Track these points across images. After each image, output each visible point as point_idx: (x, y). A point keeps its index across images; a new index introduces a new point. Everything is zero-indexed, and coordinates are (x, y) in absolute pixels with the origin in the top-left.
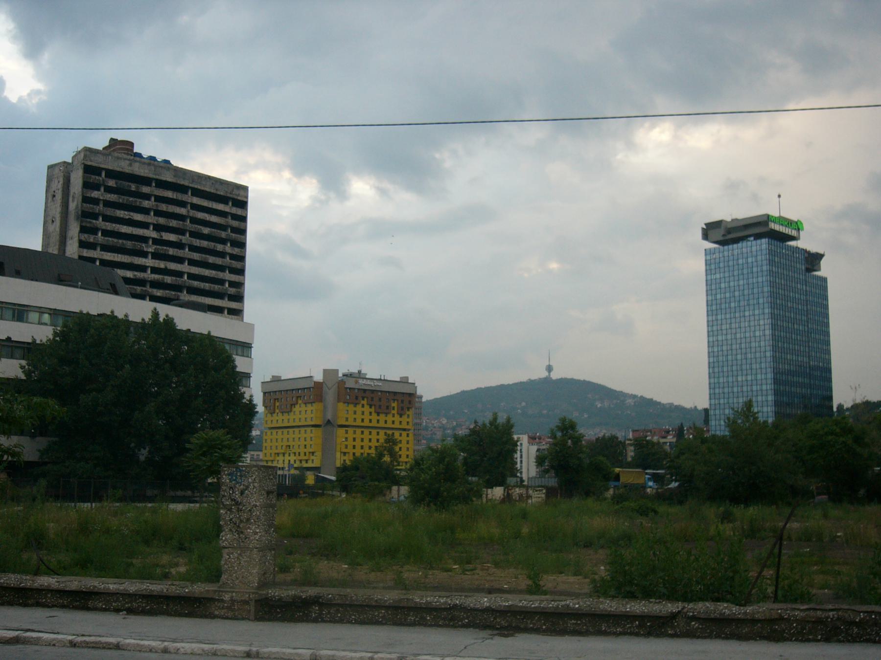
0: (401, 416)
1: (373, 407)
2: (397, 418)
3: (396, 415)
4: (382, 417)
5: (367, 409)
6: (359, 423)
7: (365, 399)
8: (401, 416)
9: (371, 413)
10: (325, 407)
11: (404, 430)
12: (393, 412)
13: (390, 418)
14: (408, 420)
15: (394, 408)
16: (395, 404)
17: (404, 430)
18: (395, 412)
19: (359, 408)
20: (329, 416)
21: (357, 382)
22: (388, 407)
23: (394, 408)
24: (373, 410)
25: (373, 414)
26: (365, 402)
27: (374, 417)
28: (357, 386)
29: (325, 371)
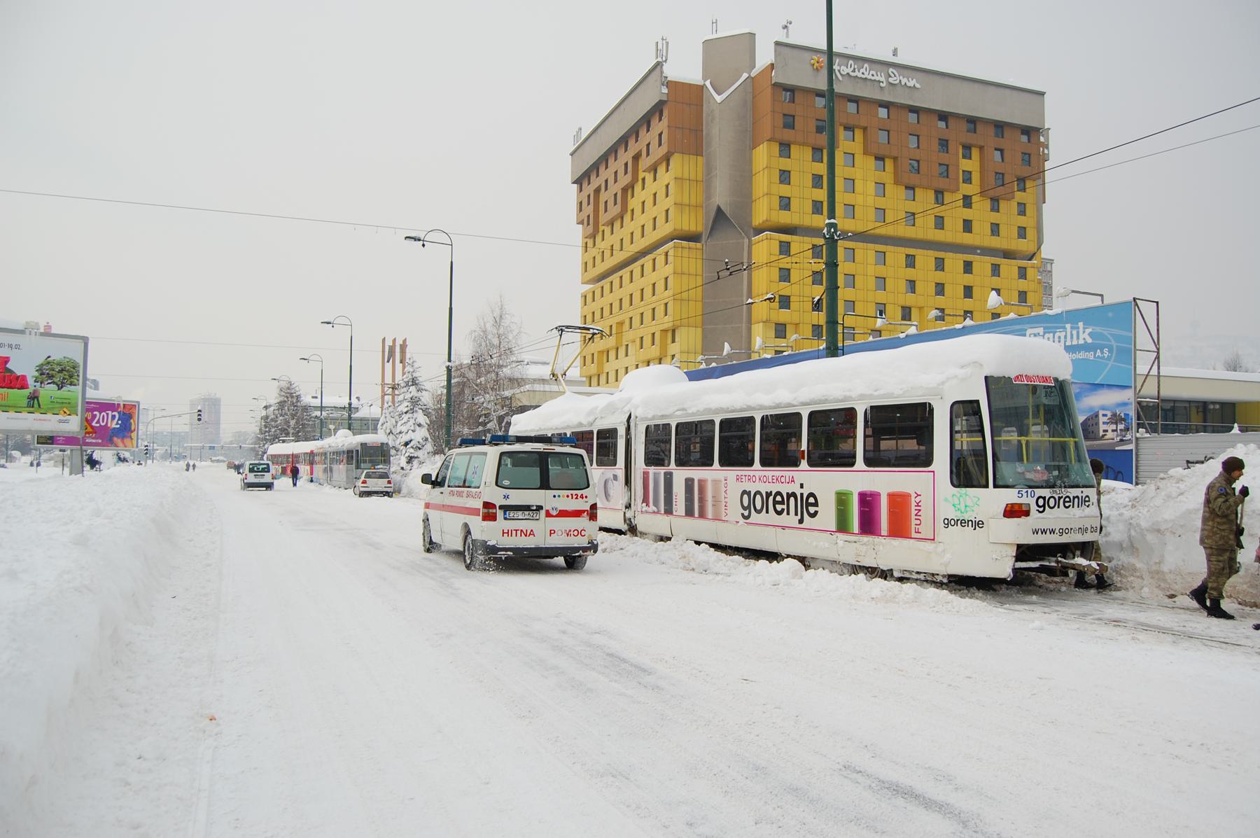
0: (995, 205)
1: (889, 164)
2: (981, 212)
7: (859, 134)
8: (995, 205)
9: (881, 186)
10: (709, 169)
11: (1008, 255)
12: (966, 189)
14: (1022, 221)
15: (968, 178)
17: (1008, 255)
18: (972, 189)
20: (721, 196)
22: (946, 170)
23: (968, 178)
24: (887, 176)
25: (890, 188)
27: (897, 201)
29: (712, 48)
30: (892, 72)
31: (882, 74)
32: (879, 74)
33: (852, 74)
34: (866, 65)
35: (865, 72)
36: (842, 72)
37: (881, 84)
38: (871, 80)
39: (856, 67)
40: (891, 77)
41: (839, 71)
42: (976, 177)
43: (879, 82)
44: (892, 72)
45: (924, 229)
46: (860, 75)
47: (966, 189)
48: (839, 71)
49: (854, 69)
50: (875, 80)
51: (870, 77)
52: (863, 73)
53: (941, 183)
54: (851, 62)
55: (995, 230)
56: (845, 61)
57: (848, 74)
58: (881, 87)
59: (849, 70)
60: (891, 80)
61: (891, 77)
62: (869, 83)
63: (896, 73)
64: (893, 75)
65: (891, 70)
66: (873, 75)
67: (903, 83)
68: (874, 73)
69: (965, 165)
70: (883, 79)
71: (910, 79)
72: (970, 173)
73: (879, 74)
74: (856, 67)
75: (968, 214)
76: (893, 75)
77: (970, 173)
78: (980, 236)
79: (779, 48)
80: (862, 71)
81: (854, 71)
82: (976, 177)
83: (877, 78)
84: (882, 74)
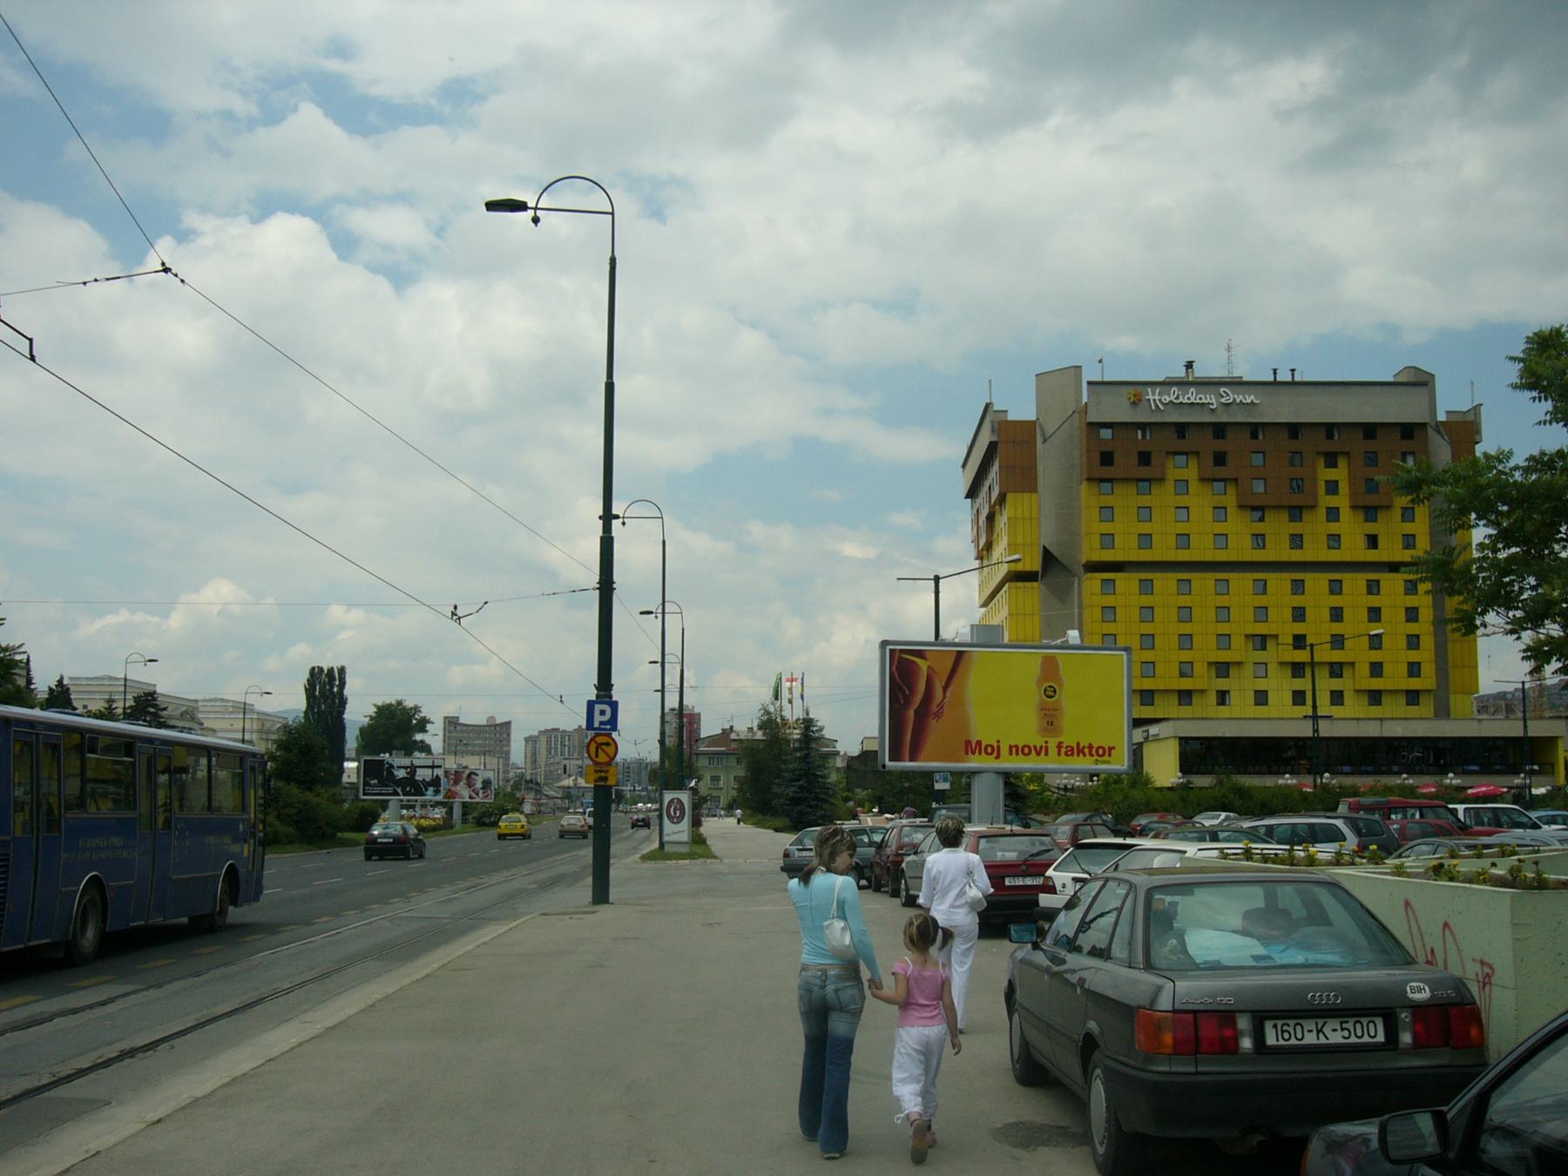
2: (1351, 528)
3: (1345, 513)
4: (1278, 528)
5: (1201, 500)
6: (1164, 550)
12: (1333, 501)
13: (1315, 527)
14: (1409, 528)
15: (1332, 487)
16: (1340, 473)
18: (1342, 501)
19: (1163, 498)
21: (1136, 402)
23: (1332, 487)
24: (1230, 500)
26: (1191, 472)
28: (1141, 417)
30: (1224, 392)
31: (1212, 396)
32: (1208, 396)
33: (1175, 401)
34: (1192, 389)
35: (1192, 396)
36: (1163, 400)
37: (1211, 406)
38: (1198, 403)
39: (1180, 393)
40: (1223, 397)
41: (1160, 400)
42: (1344, 487)
43: (1209, 404)
44: (1224, 392)
45: (1278, 550)
46: (1186, 401)
47: (1333, 501)
48: (1160, 400)
49: (1178, 395)
50: (1203, 403)
51: (1198, 401)
52: (1189, 399)
53: (1296, 500)
54: (1174, 388)
55: (1373, 542)
56: (1165, 388)
57: (1171, 402)
58: (1212, 410)
59: (1172, 398)
60: (1223, 400)
61: (1223, 397)
62: (1197, 407)
63: (1226, 390)
64: (1224, 395)
65: (1222, 390)
66: (1201, 399)
67: (1238, 401)
68: (1203, 396)
69: (1331, 474)
70: (1214, 401)
71: (1247, 397)
72: (1336, 482)
73: (1208, 396)
74: (1180, 393)
75: (1334, 528)
76: (1224, 395)
77: (1336, 482)
78: (1354, 550)
79: (1091, 387)
80: (1186, 397)
81: (1177, 398)
82: (1344, 487)
83: (1209, 400)
84: (1212, 396)
